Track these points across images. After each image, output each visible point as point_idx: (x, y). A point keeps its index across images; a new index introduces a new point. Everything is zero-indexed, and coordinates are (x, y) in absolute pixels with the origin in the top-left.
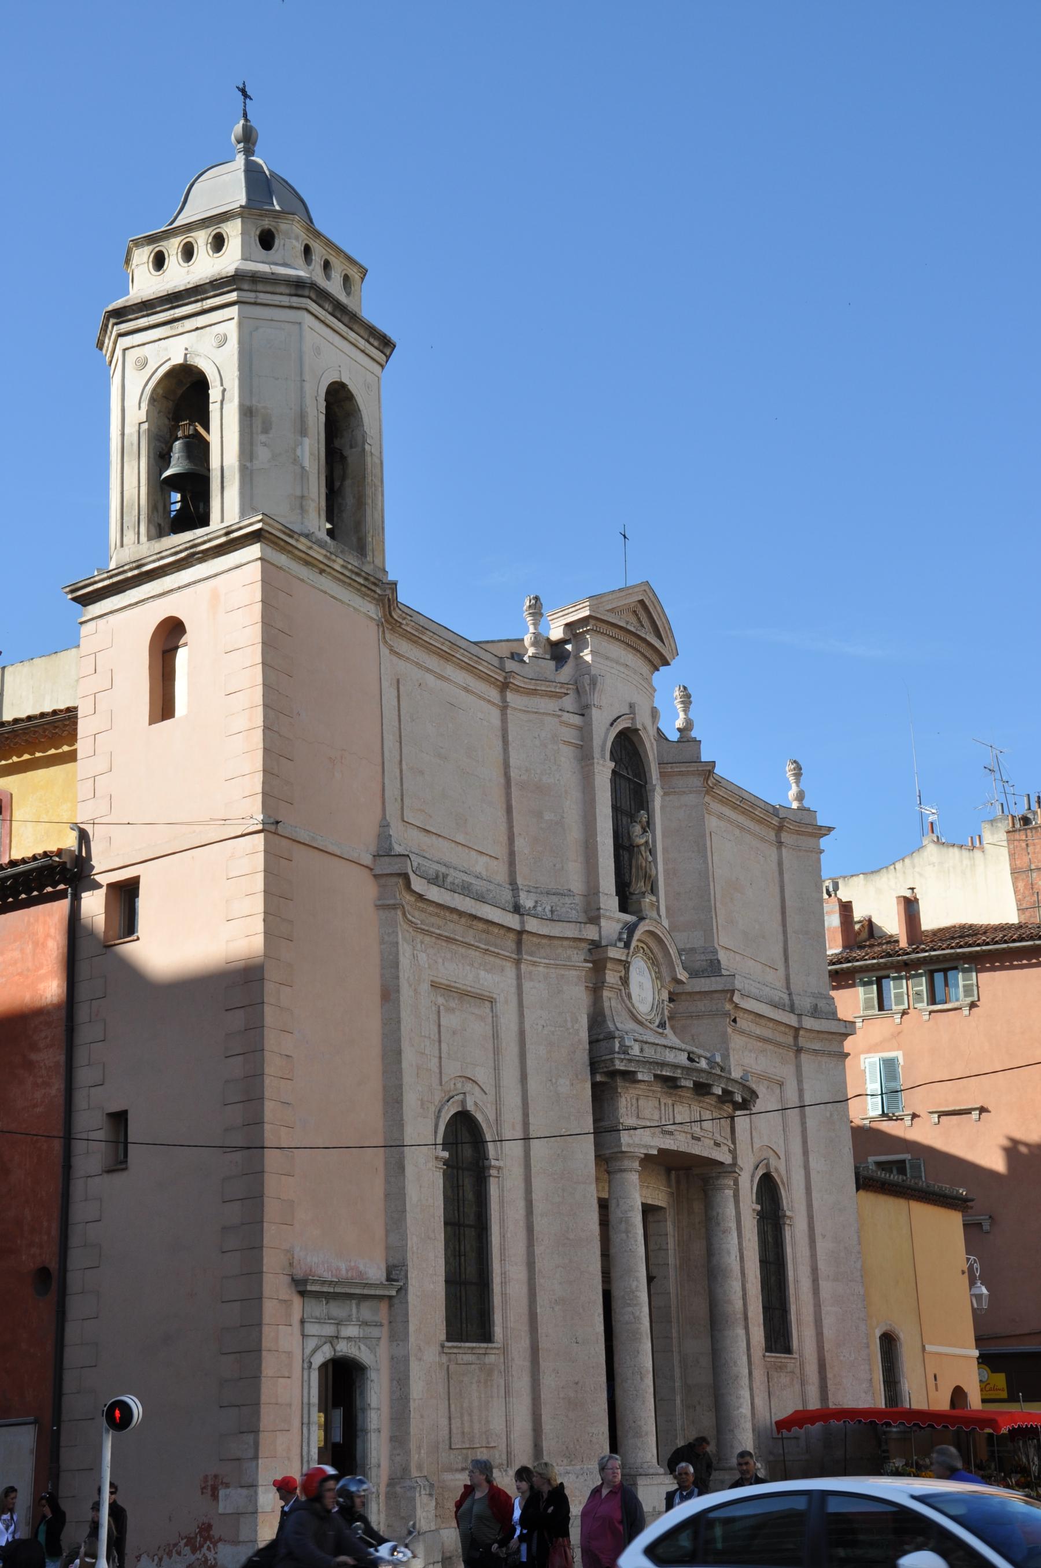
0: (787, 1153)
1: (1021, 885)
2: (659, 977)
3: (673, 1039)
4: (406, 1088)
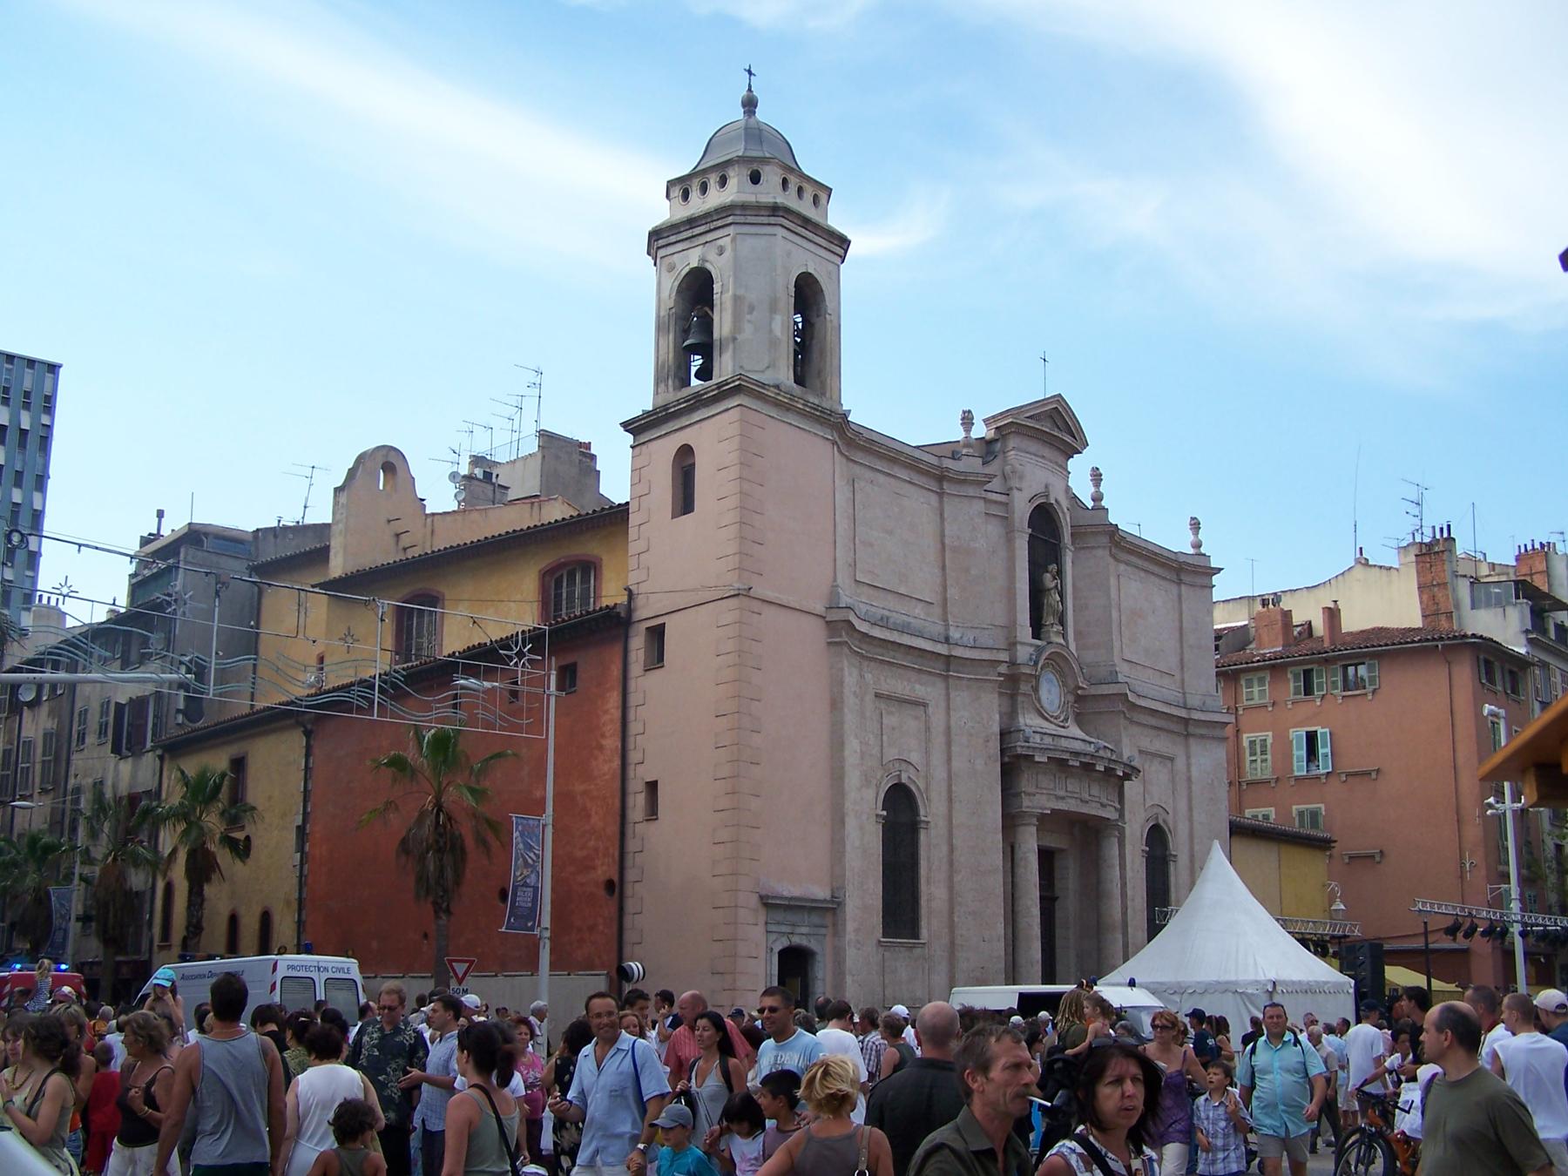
0: (1175, 809)
1: (1425, 597)
2: (1065, 684)
3: (1075, 731)
4: (848, 768)
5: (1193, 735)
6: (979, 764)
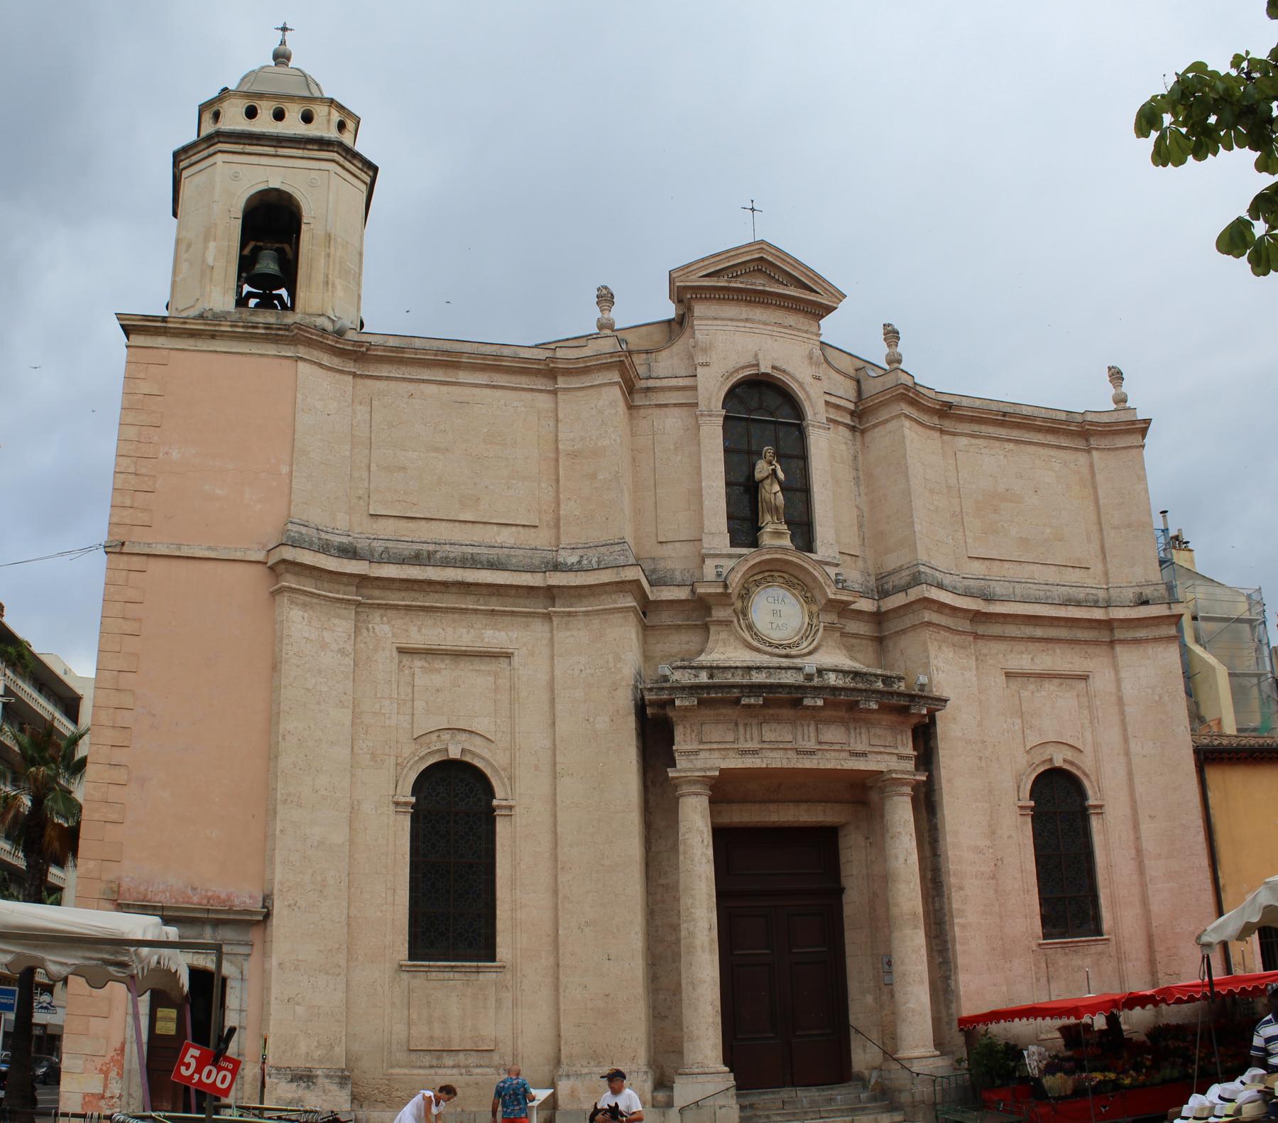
0: (1096, 747)
2: (809, 600)
5: (1121, 641)
6: (602, 722)
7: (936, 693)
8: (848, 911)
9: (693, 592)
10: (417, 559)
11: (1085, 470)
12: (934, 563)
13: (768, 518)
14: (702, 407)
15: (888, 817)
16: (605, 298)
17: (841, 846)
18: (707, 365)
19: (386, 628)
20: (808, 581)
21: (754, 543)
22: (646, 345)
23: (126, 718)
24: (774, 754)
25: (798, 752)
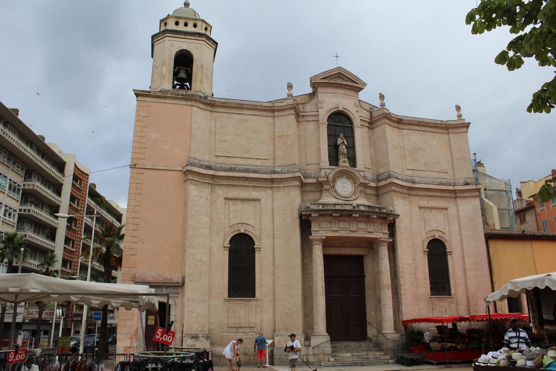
2: (354, 183)
7: (396, 213)
8: (366, 283)
9: (317, 180)
10: (230, 170)
11: (447, 140)
12: (395, 171)
13: (341, 157)
14: (320, 121)
15: (380, 253)
16: (290, 87)
17: (364, 262)
18: (322, 108)
19: (221, 191)
20: (354, 176)
21: (337, 165)
22: (303, 102)
23: (137, 221)
24: (343, 232)
25: (351, 231)
